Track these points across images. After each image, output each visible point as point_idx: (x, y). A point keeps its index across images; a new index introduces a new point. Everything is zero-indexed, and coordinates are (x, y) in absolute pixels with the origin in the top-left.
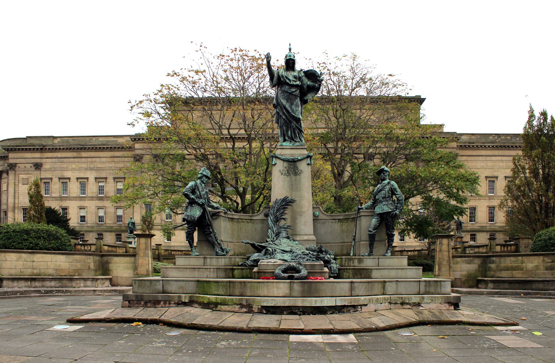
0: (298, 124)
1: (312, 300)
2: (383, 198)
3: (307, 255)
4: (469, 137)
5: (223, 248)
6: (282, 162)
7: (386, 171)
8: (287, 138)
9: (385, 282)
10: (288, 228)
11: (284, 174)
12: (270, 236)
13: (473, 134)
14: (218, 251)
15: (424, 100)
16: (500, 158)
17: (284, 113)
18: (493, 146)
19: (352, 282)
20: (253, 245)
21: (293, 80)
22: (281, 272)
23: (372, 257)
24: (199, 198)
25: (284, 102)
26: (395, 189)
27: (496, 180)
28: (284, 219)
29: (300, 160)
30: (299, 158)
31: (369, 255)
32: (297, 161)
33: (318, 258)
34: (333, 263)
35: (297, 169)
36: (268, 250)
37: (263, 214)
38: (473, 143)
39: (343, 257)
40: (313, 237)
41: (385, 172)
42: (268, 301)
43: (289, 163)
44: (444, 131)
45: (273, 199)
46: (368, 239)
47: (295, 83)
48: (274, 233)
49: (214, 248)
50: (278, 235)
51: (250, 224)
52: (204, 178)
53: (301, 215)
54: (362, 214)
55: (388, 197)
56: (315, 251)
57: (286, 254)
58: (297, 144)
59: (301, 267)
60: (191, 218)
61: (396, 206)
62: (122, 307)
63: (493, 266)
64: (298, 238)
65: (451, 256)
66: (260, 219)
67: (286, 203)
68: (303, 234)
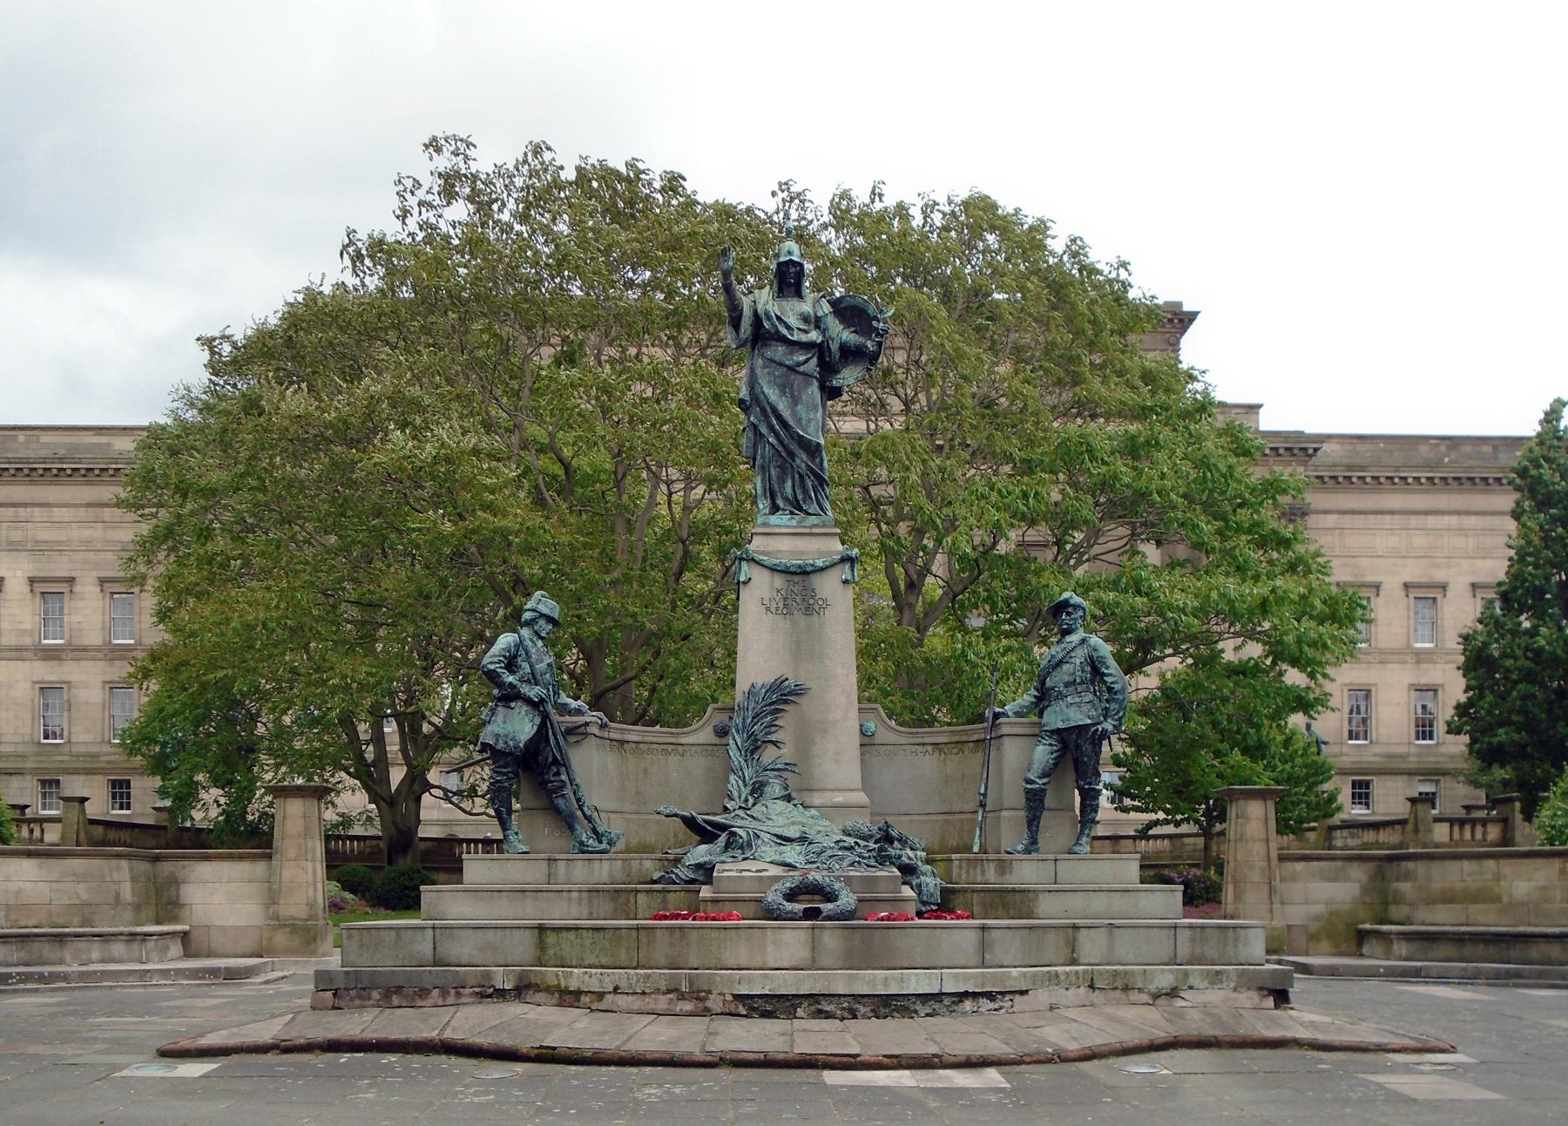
0: (813, 462)
1: (874, 975)
2: (1067, 685)
3: (850, 848)
4: (1348, 447)
5: (600, 829)
6: (766, 574)
7: (1077, 607)
8: (780, 502)
9: (1076, 927)
10: (785, 770)
12: (735, 794)
13: (1361, 438)
14: (584, 838)
15: (1191, 317)
16: (1453, 520)
17: (771, 428)
18: (1430, 479)
19: (983, 928)
20: (690, 822)
21: (799, 329)
22: (781, 900)
23: (1034, 855)
24: (528, 682)
26: (1102, 660)
27: (1439, 597)
28: (774, 743)
29: (822, 569)
30: (819, 563)
31: (1027, 851)
33: (882, 859)
34: (924, 874)
35: (812, 597)
36: (734, 834)
38: (1362, 468)
39: (954, 856)
40: (861, 798)
41: (1070, 610)
42: (750, 980)
43: (789, 577)
44: (1262, 428)
45: (742, 685)
46: (1022, 801)
47: (804, 338)
48: (745, 786)
49: (571, 828)
50: (758, 789)
51: (673, 760)
52: (542, 622)
53: (825, 732)
54: (1005, 730)
55: (1082, 683)
56: (871, 836)
57: (787, 848)
58: (813, 520)
59: (837, 886)
60: (506, 743)
61: (1106, 709)
62: (313, 1008)
63: (1405, 887)
64: (817, 799)
65: (1274, 854)
66: (702, 742)
67: (782, 696)
68: (829, 786)
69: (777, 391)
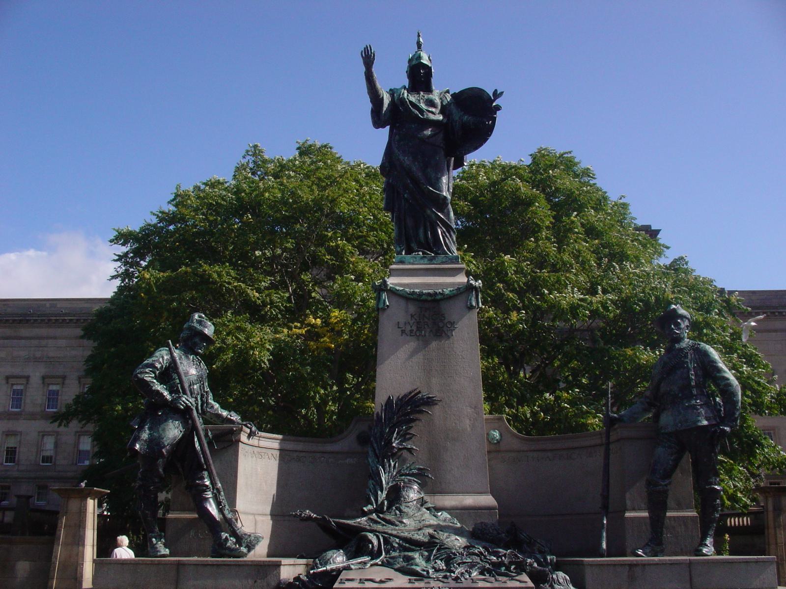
6: (402, 303)
8: (414, 245)
25: (406, 160)
30: (447, 291)
45: (381, 397)
69: (411, 158)
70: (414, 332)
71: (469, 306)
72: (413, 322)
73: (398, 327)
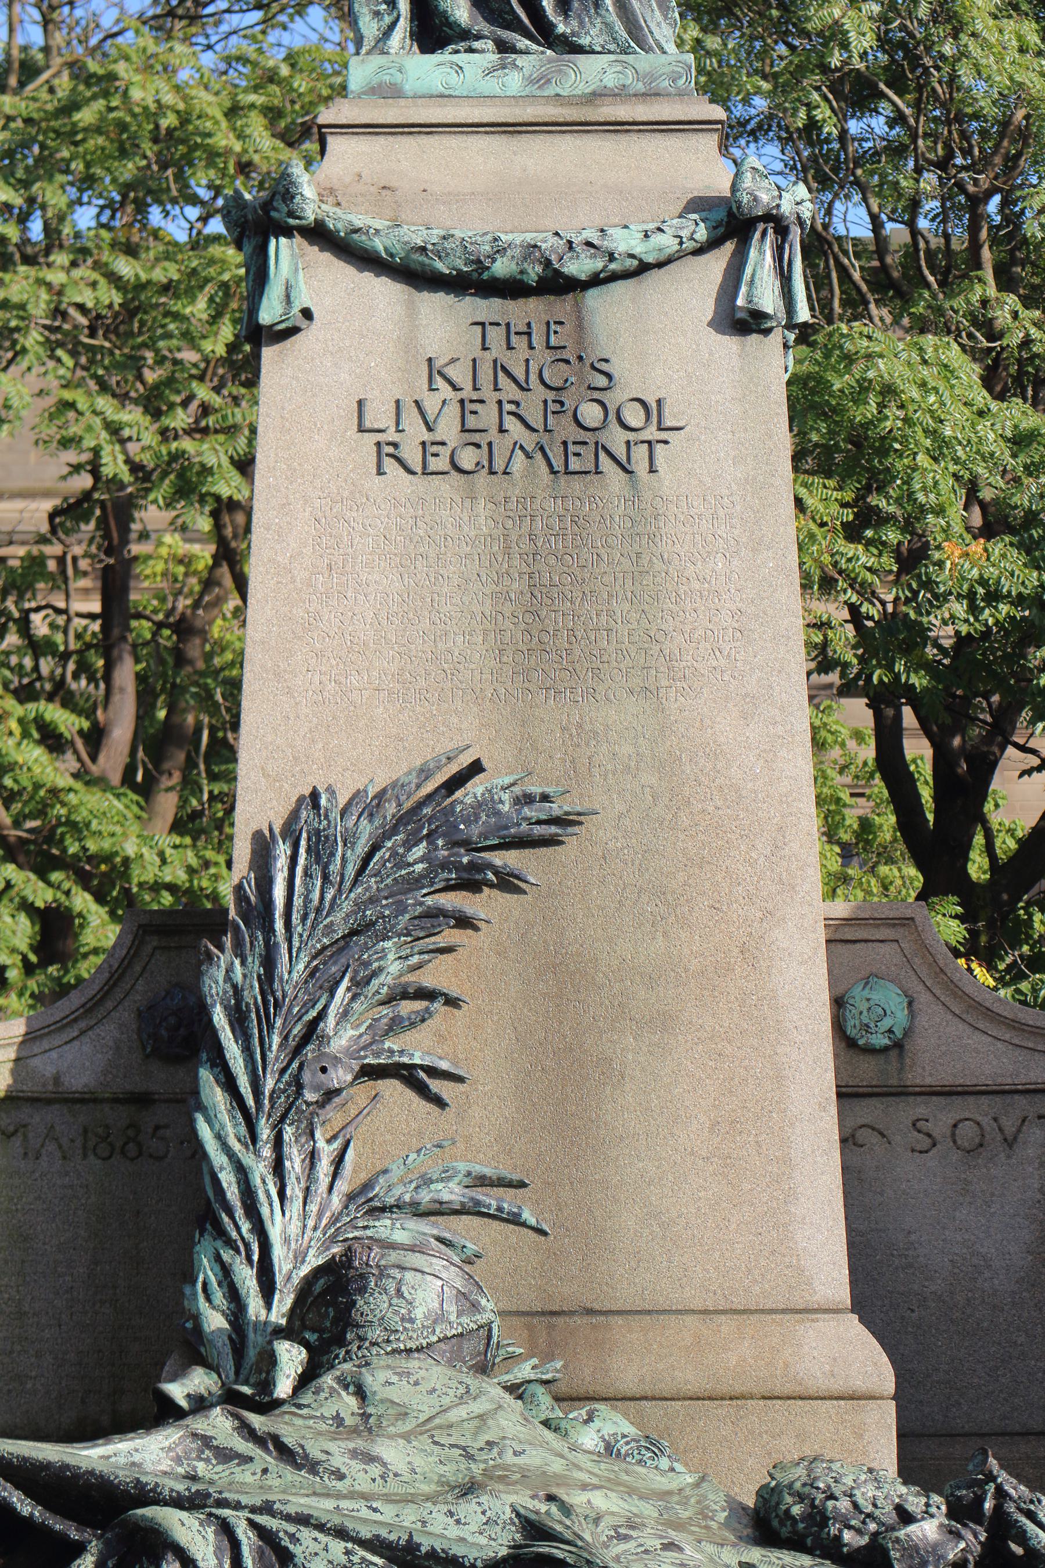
11: (413, 457)
32: (596, 281)
35: (597, 395)
37: (125, 1015)
70: (445, 452)
71: (740, 315)
72: (438, 397)
73: (361, 430)
